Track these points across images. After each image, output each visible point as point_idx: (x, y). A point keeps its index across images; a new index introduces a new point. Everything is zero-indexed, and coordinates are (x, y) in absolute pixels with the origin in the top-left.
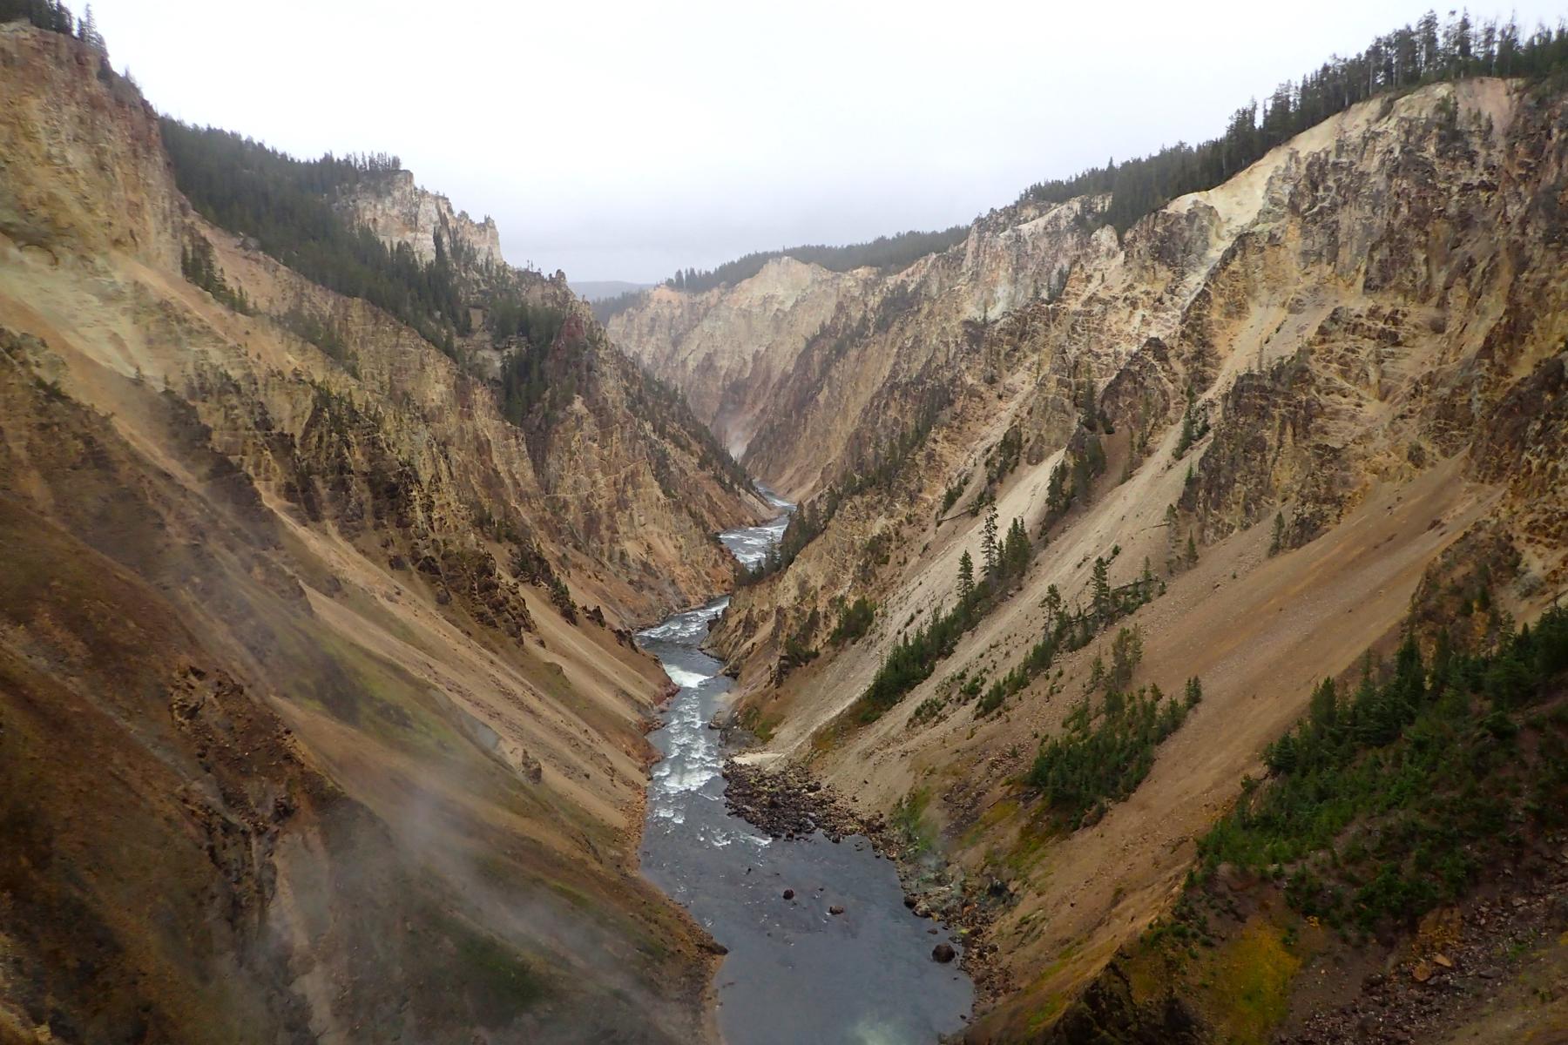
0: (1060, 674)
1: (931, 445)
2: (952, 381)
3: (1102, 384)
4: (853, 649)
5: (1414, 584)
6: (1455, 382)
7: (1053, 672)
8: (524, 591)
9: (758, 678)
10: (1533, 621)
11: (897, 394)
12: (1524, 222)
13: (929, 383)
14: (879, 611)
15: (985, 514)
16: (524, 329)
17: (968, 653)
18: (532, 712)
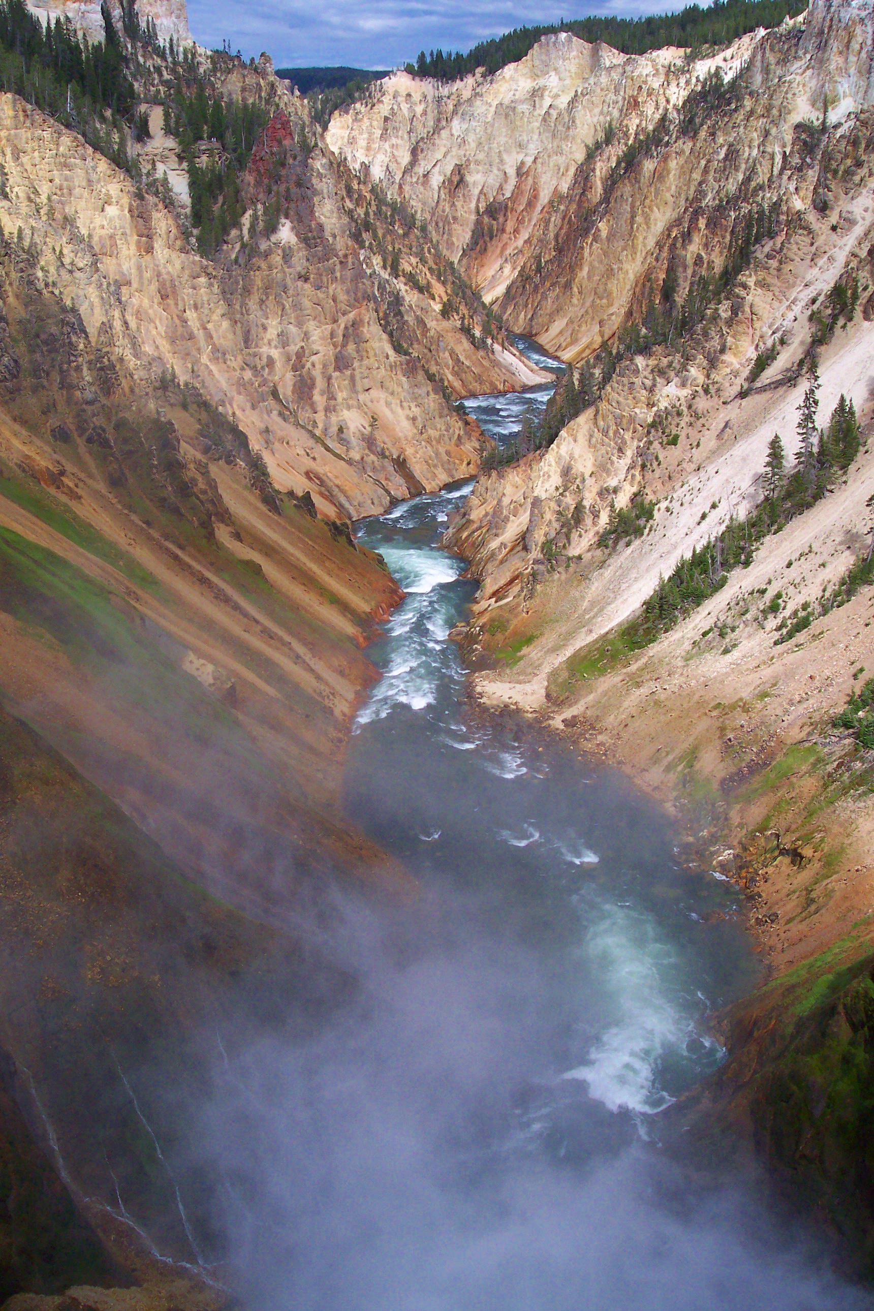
4: (626, 554)
13: (745, 208)
14: (663, 505)
15: (804, 385)
16: (218, 133)
17: (772, 558)
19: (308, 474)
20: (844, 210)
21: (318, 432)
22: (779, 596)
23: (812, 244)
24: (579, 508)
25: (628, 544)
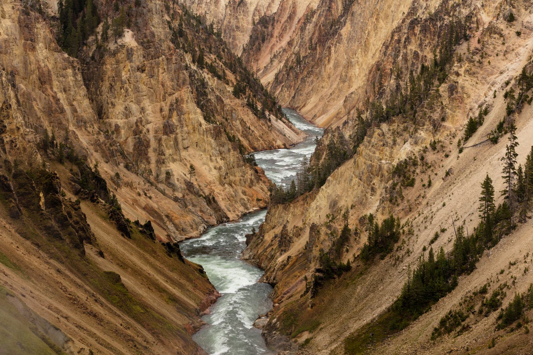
1: (453, 77)
2: (469, 17)
8: (85, 207)
9: (297, 286)
11: (417, 30)
13: (447, 20)
15: (505, 141)
18: (95, 316)
20: (525, 21)
21: (152, 178)
22: (496, 294)
23: (503, 44)
24: (346, 230)
25: (382, 258)
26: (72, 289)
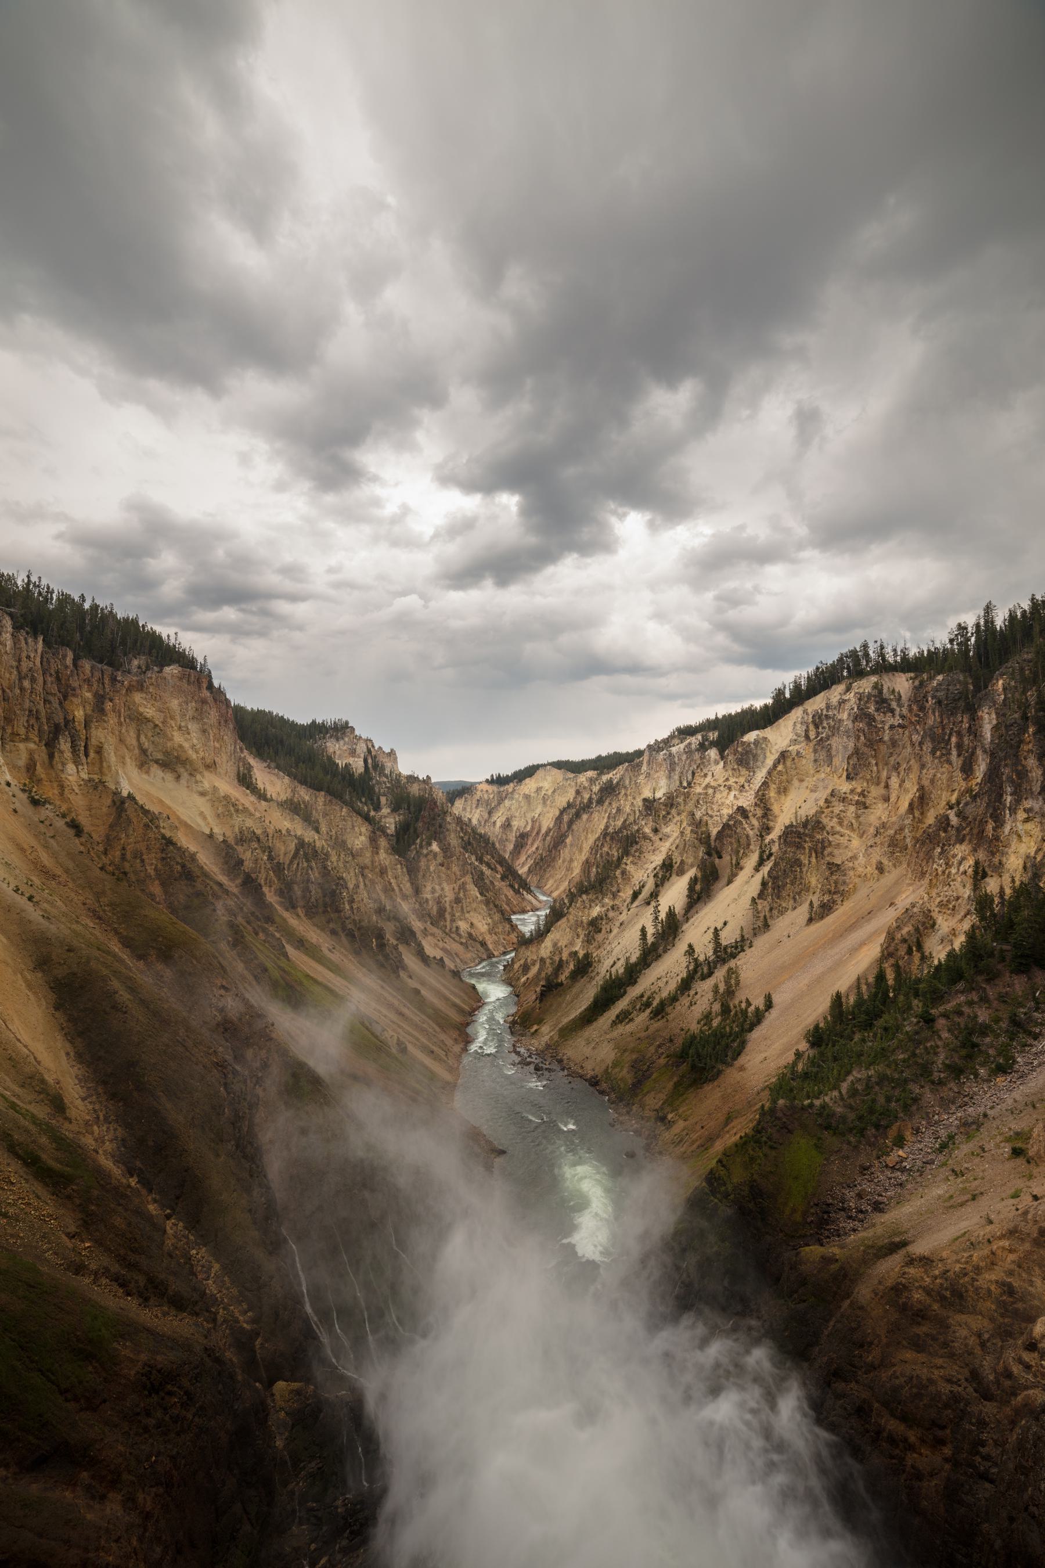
0: (696, 993)
1: (624, 866)
2: (638, 831)
3: (714, 831)
5: (882, 938)
6: (896, 827)
7: (692, 992)
8: (401, 948)
10: (943, 956)
11: (608, 839)
12: (921, 743)
15: (653, 904)
17: (646, 982)
19: (443, 949)
22: (649, 998)
24: (561, 960)
26: (390, 999)
